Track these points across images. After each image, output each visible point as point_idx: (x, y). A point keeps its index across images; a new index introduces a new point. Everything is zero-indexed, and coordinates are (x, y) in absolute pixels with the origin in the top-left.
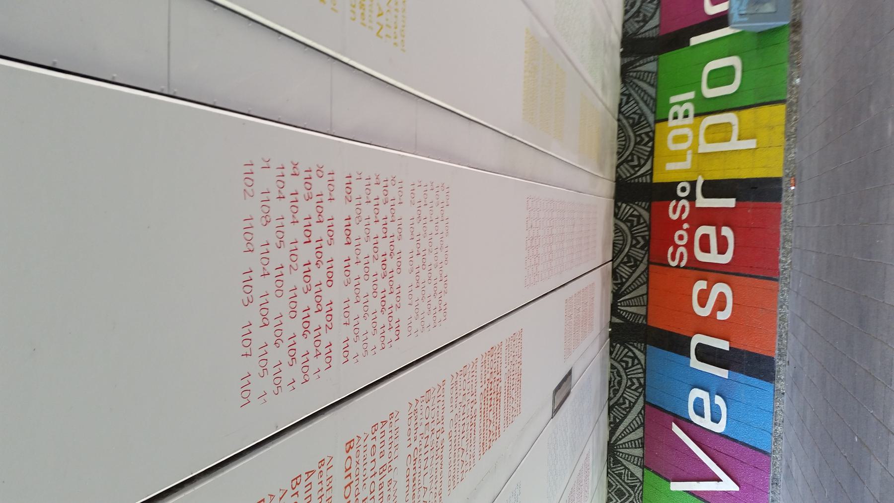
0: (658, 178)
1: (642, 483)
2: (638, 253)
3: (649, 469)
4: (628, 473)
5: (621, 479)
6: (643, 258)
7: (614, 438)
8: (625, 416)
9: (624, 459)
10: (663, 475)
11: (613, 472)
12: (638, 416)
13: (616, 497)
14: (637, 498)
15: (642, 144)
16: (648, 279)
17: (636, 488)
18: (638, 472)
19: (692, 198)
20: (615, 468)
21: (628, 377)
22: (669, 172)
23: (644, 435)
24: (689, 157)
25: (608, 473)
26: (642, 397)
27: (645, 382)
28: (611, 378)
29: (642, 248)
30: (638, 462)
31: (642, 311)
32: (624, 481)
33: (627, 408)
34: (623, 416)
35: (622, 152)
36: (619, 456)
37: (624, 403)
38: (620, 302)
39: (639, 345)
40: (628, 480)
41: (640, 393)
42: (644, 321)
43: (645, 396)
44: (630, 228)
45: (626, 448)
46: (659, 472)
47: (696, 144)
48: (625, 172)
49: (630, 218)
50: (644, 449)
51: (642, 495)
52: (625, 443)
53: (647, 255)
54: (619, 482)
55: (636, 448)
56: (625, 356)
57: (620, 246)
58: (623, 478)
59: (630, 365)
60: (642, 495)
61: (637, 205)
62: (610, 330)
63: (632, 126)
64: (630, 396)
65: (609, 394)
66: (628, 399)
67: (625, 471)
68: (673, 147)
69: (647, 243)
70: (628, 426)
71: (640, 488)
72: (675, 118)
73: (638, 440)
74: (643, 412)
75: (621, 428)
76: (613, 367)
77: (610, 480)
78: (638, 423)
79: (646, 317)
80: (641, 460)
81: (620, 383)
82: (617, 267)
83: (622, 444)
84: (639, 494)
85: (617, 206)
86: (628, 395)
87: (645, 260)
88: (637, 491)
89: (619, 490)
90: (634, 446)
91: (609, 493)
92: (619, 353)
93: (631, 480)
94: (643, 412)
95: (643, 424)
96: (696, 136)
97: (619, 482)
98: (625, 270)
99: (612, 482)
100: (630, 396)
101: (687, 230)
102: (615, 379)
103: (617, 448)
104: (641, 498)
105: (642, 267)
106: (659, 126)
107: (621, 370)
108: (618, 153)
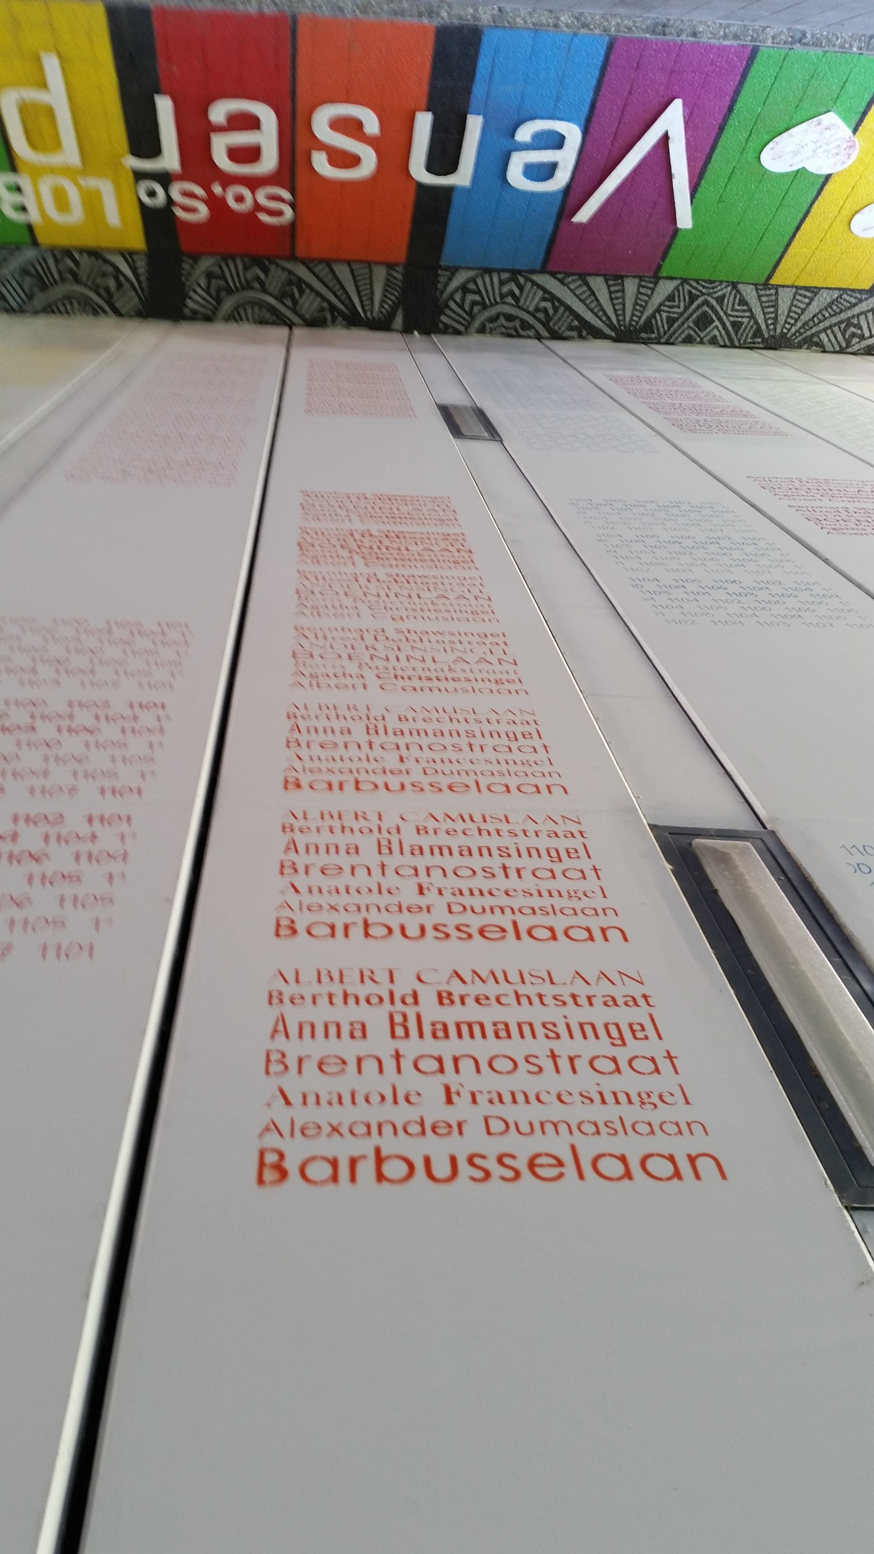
0: (136, 240)
1: (685, 281)
2: (276, 278)
3: (659, 267)
4: (666, 306)
5: (677, 319)
6: (284, 269)
7: (607, 331)
8: (568, 308)
9: (642, 313)
10: (667, 240)
11: (665, 333)
13: (709, 329)
14: (711, 291)
15: (75, 268)
16: (321, 261)
17: (694, 291)
18: (666, 288)
19: (165, 179)
21: (498, 299)
22: (123, 218)
23: (600, 275)
24: (92, 182)
25: (667, 343)
26: (535, 277)
27: (508, 271)
29: (266, 271)
30: (648, 288)
31: (380, 274)
32: (681, 314)
33: (553, 304)
35: (90, 305)
36: (637, 323)
38: (365, 312)
39: (442, 279)
42: (397, 268)
43: (533, 272)
44: (230, 292)
45: (624, 310)
46: (662, 248)
47: (67, 171)
48: (129, 300)
49: (213, 292)
50: (627, 276)
51: (705, 281)
52: (615, 311)
53: (278, 261)
54: (683, 324)
55: (623, 291)
56: (461, 306)
57: (264, 310)
58: (675, 315)
59: (477, 298)
60: (705, 281)
61: (187, 279)
62: (416, 333)
63: (44, 287)
64: (533, 299)
65: (529, 337)
66: (538, 303)
67: (664, 311)
68: (77, 214)
69: (259, 261)
71: (694, 284)
72: (24, 209)
73: (609, 286)
74: (560, 276)
75: (589, 316)
76: (482, 330)
77: (680, 339)
78: (580, 286)
79: (390, 266)
80: (645, 281)
81: (510, 318)
82: (301, 316)
83: (617, 316)
84: (704, 287)
85: (194, 317)
87: (288, 265)
88: (700, 291)
89: (696, 323)
90: (619, 294)
91: (701, 342)
92: (456, 317)
93: (679, 301)
95: (582, 276)
96: (52, 170)
97: (683, 324)
98: (309, 304)
99: (683, 336)
100: (533, 300)
101: (224, 188)
104: (711, 282)
105: (301, 271)
106: (42, 238)
107: (487, 314)
108: (95, 313)
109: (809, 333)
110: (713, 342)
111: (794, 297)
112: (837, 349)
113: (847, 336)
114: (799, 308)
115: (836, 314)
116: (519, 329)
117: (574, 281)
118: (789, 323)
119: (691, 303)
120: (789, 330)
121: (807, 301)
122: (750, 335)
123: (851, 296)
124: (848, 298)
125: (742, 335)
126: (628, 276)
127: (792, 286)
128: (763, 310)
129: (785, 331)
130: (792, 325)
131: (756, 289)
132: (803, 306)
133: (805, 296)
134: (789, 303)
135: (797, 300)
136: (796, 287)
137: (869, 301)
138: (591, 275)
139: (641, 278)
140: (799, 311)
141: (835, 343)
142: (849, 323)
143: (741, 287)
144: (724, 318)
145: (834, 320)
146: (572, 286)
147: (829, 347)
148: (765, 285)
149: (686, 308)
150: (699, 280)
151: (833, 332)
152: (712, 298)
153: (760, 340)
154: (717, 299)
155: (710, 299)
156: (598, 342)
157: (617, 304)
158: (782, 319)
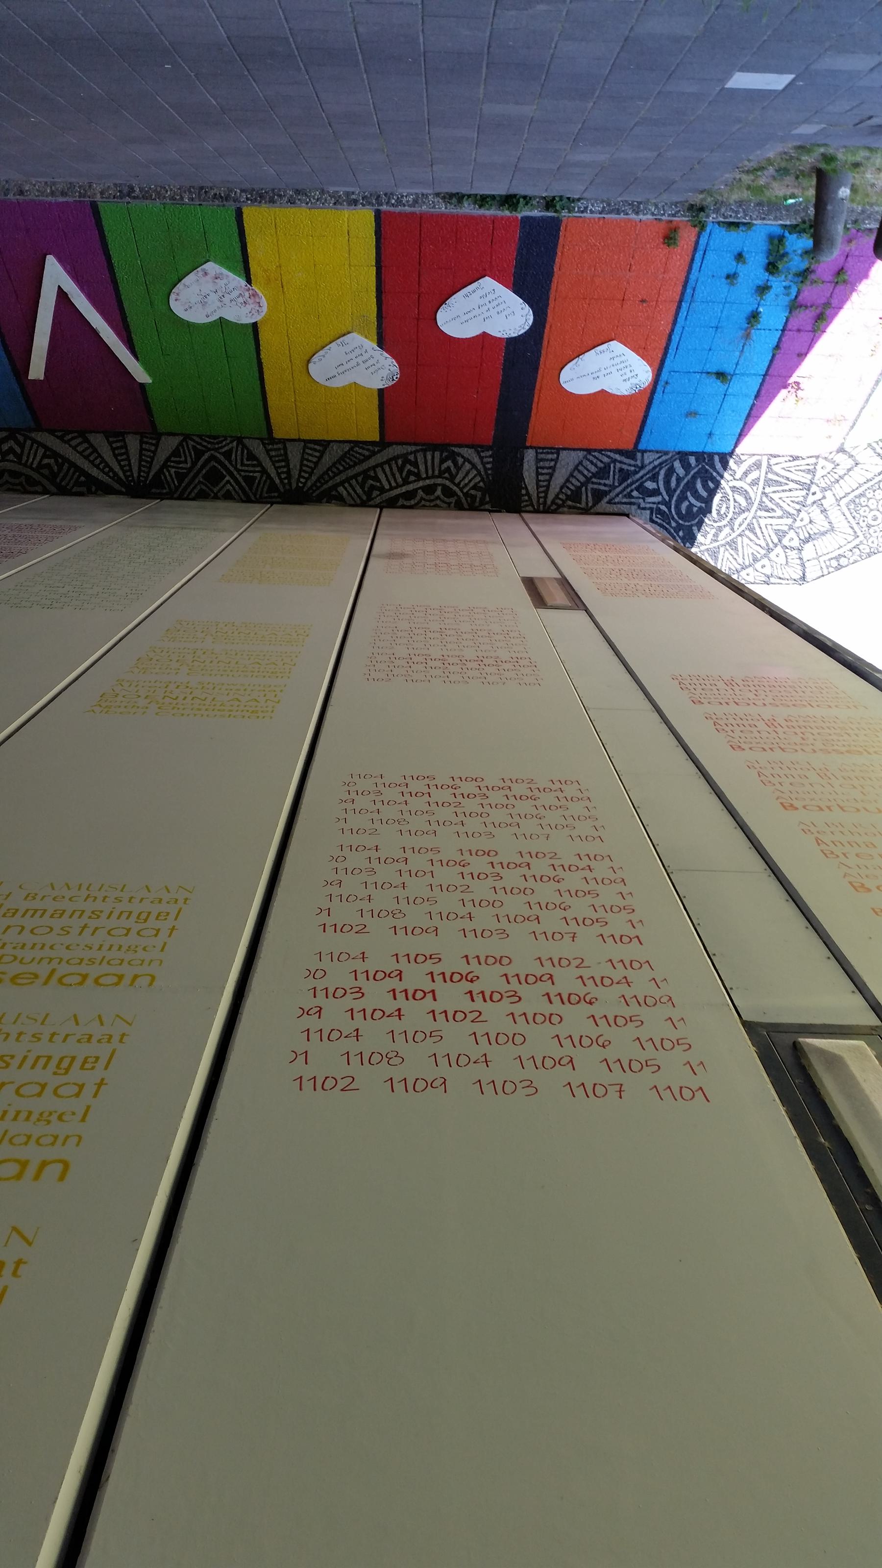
1: (187, 437)
4: (173, 462)
5: (186, 475)
7: (117, 486)
8: (72, 464)
9: (150, 468)
11: (177, 488)
12: (68, 442)
17: (198, 446)
18: (168, 445)
20: (169, 486)
25: (180, 498)
26: (33, 435)
28: (9, 490)
32: (190, 470)
33: (56, 462)
34: (72, 470)
37: (48, 466)
40: (186, 462)
41: (26, 438)
43: (31, 430)
45: (130, 465)
52: (122, 467)
58: (185, 471)
60: (209, 437)
66: (41, 460)
70: (90, 461)
73: (110, 443)
74: (59, 434)
75: (94, 472)
77: (193, 494)
81: (14, 474)
84: (209, 443)
86: (34, 459)
91: (216, 497)
94: (59, 434)
95: (82, 434)
99: (196, 491)
102: (7, 482)
103: (133, 480)
104: (215, 437)
109: (325, 486)
110: (228, 497)
111: (304, 451)
112: (358, 501)
113: (366, 489)
114: (310, 461)
115: (350, 467)
116: (27, 486)
117: (73, 438)
118: (304, 477)
119: (198, 458)
120: (305, 484)
121: (317, 454)
122: (265, 490)
123: (364, 449)
124: (361, 451)
125: (257, 490)
126: (129, 433)
127: (299, 440)
128: (274, 465)
129: (300, 485)
130: (307, 479)
131: (264, 444)
132: (315, 460)
133: (315, 450)
134: (299, 456)
135: (308, 454)
136: (304, 441)
137: (382, 453)
138: (91, 432)
139: (142, 435)
140: (312, 465)
141: (355, 496)
142: (365, 472)
143: (246, 441)
144: (235, 473)
145: (350, 473)
146: (74, 443)
147: (349, 500)
148: (269, 439)
149: (194, 464)
150: (203, 435)
151: (351, 485)
152: (220, 453)
153: (276, 494)
154: (223, 454)
155: (218, 455)
156: (113, 498)
157: (122, 460)
158: (295, 473)
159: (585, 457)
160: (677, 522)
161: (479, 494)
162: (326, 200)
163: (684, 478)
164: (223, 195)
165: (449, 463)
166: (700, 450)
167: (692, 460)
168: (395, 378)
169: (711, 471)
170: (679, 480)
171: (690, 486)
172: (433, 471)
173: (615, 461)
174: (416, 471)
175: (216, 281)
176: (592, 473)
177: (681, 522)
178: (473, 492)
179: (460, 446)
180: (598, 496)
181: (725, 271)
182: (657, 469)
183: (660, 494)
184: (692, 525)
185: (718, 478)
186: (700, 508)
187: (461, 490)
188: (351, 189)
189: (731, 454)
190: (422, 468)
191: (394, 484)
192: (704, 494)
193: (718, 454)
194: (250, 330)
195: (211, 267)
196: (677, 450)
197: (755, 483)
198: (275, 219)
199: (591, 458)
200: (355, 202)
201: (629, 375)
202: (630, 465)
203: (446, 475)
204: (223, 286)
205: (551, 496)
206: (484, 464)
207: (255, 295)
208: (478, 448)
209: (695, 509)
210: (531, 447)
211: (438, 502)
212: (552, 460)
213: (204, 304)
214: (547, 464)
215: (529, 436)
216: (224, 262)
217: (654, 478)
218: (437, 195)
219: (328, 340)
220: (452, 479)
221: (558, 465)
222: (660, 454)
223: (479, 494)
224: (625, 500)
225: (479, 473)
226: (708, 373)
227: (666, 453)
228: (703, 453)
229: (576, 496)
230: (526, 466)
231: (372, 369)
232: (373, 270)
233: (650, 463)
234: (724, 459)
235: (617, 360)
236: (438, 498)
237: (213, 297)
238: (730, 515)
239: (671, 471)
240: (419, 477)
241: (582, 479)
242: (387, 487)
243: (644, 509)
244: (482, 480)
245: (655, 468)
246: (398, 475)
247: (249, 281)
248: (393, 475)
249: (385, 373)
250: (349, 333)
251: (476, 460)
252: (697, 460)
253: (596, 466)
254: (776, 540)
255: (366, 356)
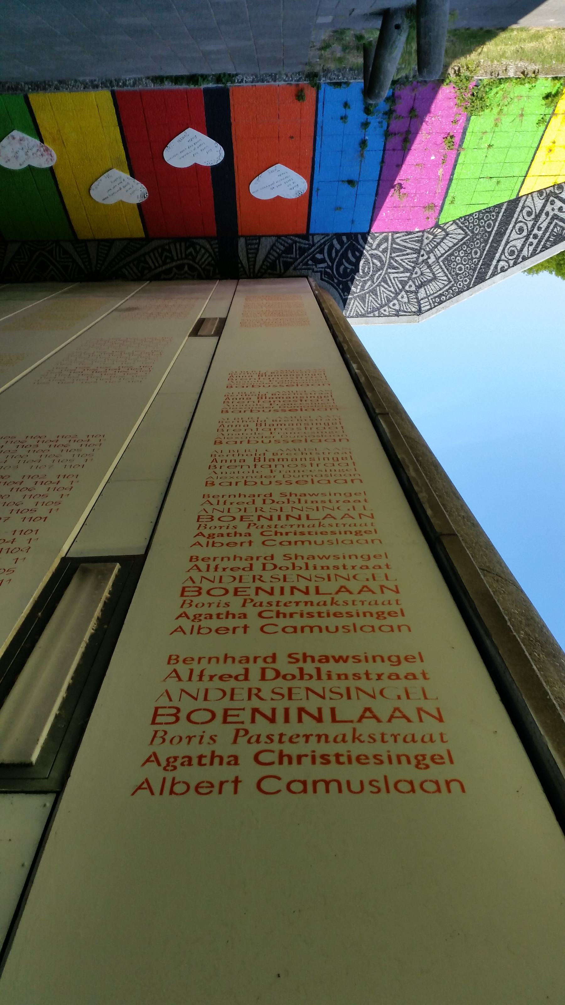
129: (98, 269)
132: (105, 252)
148: (75, 240)
159: (277, 241)
160: (338, 279)
161: (212, 269)
162: (78, 86)
163: (339, 251)
164: (13, 87)
165: (191, 249)
166: (349, 232)
167: (344, 238)
168: (146, 196)
169: (357, 244)
170: (337, 252)
171: (344, 256)
172: (181, 255)
173: (296, 242)
174: (170, 256)
175: (22, 142)
176: (282, 250)
177: (340, 279)
178: (208, 267)
179: (197, 238)
180: (287, 265)
181: (339, 115)
182: (323, 246)
183: (326, 262)
184: (347, 281)
185: (362, 249)
186: (352, 269)
187: (200, 266)
188: (93, 78)
189: (369, 232)
190: (174, 253)
191: (157, 265)
192: (353, 260)
193: (361, 234)
194: (49, 173)
195: (16, 133)
196: (334, 232)
197: (385, 251)
198: (50, 100)
199: (281, 241)
200: (96, 87)
201: (293, 185)
202: (305, 244)
203: (190, 257)
204: (26, 145)
205: (257, 267)
206: (213, 249)
207: (47, 150)
208: (208, 239)
209: (349, 270)
210: (242, 236)
211: (186, 275)
212: (256, 244)
213: (17, 158)
214: (253, 247)
215: (239, 229)
216: (24, 130)
217: (321, 252)
218: (148, 78)
219: (99, 175)
220: (194, 259)
221: (260, 247)
222: (324, 236)
223: (212, 269)
224: (304, 267)
225: (210, 255)
226: (343, 181)
227: (327, 235)
228: (351, 233)
229: (273, 266)
230: (240, 249)
231: (130, 192)
232: (118, 129)
233: (318, 242)
234: (365, 237)
235: (283, 176)
236: (186, 272)
237: (21, 153)
238: (371, 273)
239: (331, 246)
240: (173, 260)
241: (276, 255)
242: (153, 267)
243: (317, 272)
244: (213, 259)
245: (321, 245)
246: (159, 259)
247: (42, 141)
248: (156, 259)
249: (139, 193)
250: (111, 169)
251: (208, 246)
252: (347, 238)
253: (284, 246)
254: (401, 287)
255: (124, 184)
